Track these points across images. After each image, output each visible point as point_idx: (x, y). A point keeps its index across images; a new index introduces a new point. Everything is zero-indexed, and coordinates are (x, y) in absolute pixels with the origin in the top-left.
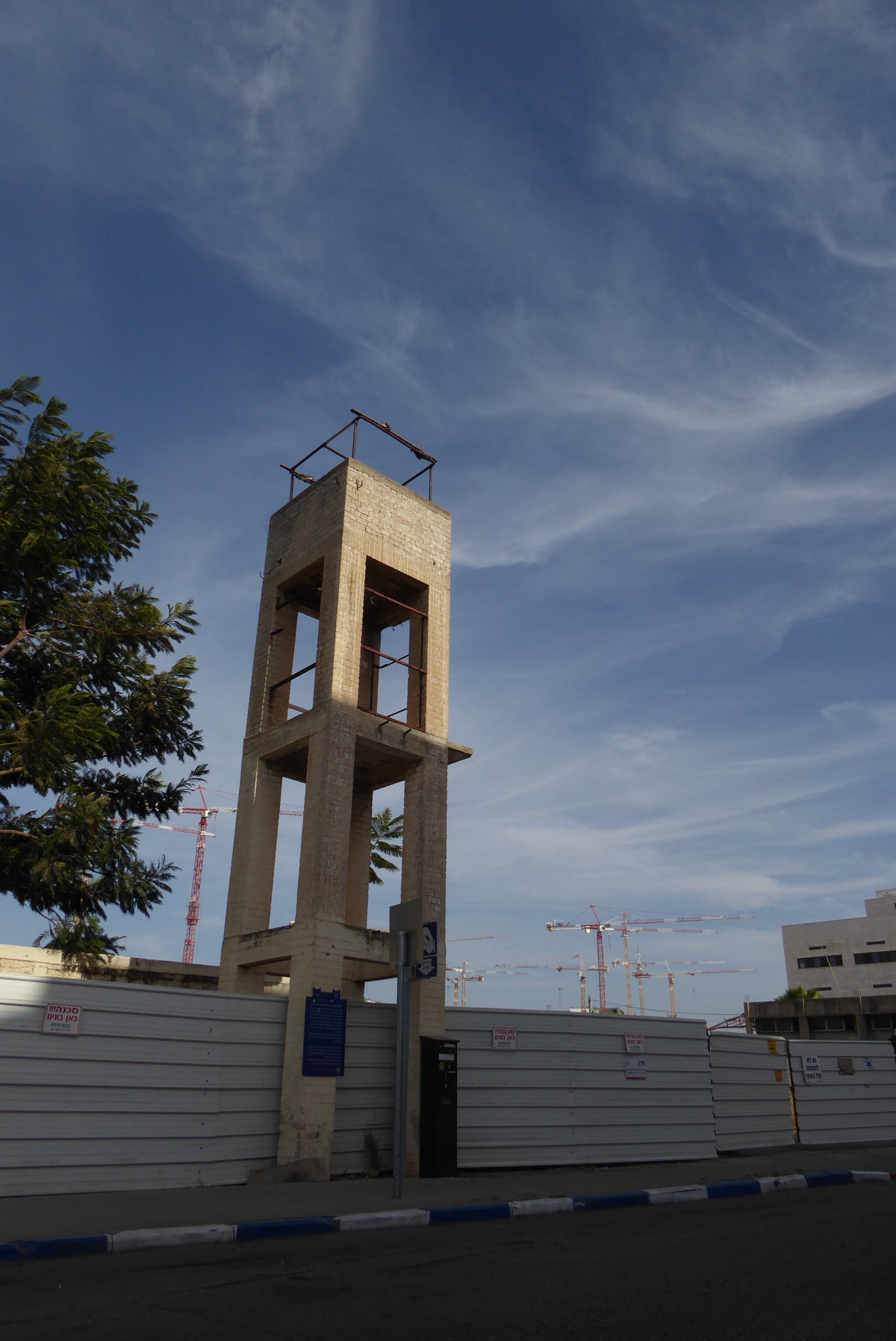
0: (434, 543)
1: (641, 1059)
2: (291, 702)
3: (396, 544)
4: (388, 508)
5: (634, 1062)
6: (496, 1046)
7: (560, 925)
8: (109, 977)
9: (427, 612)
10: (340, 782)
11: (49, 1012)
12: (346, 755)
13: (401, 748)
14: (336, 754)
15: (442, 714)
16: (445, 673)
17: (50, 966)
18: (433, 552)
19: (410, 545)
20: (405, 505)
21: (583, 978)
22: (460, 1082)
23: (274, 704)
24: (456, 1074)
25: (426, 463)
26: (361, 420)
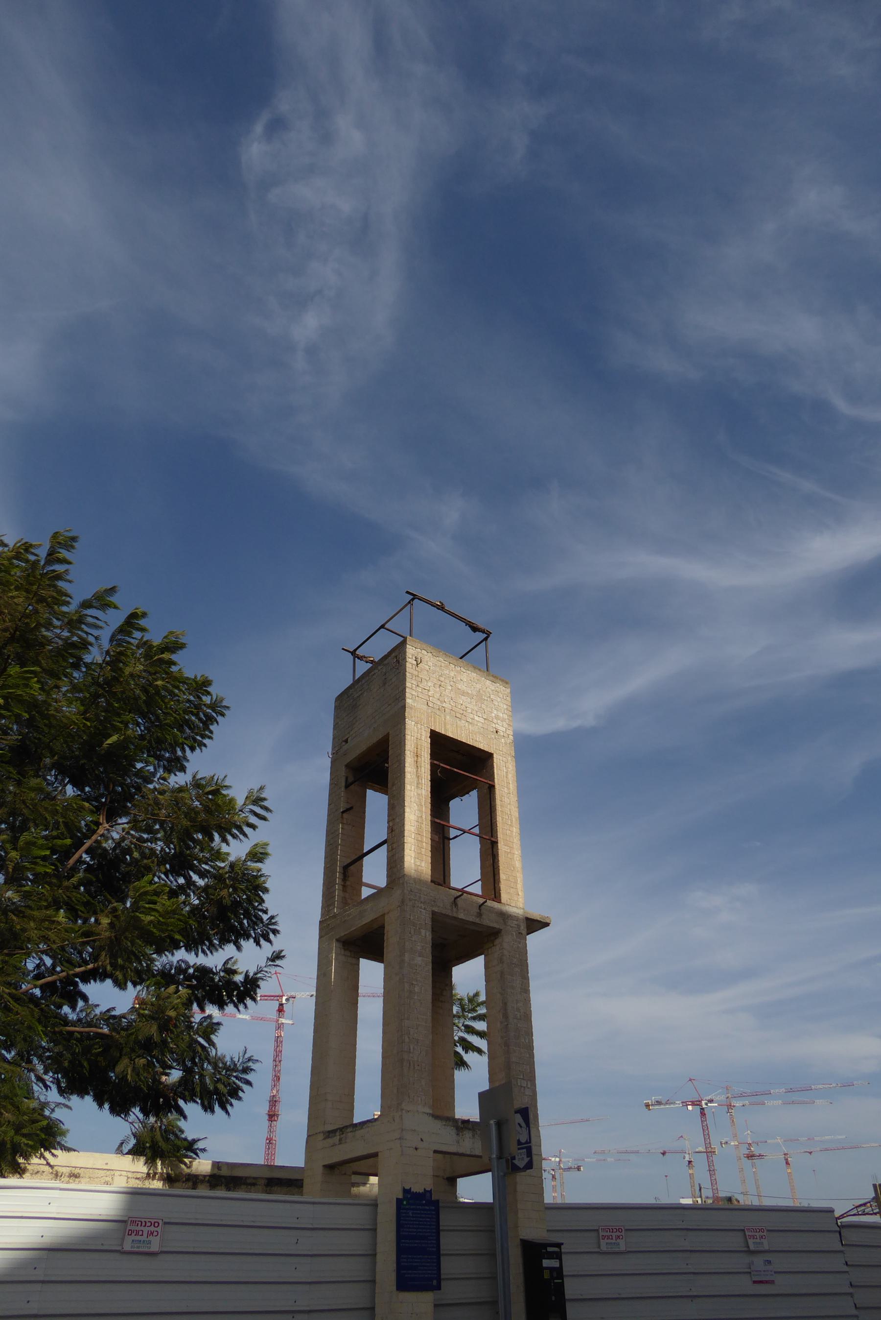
0: (495, 712)
2: (364, 880)
3: (459, 716)
4: (447, 681)
5: (758, 1262)
6: (604, 1248)
7: (659, 1103)
8: (190, 1184)
9: (493, 781)
10: (419, 960)
11: (129, 1228)
12: (423, 931)
13: (477, 921)
14: (412, 932)
15: (516, 883)
16: (516, 841)
17: (130, 1175)
18: (495, 721)
20: (464, 677)
21: (690, 1162)
22: (569, 1293)
23: (348, 883)
24: (562, 1284)
26: (416, 600)
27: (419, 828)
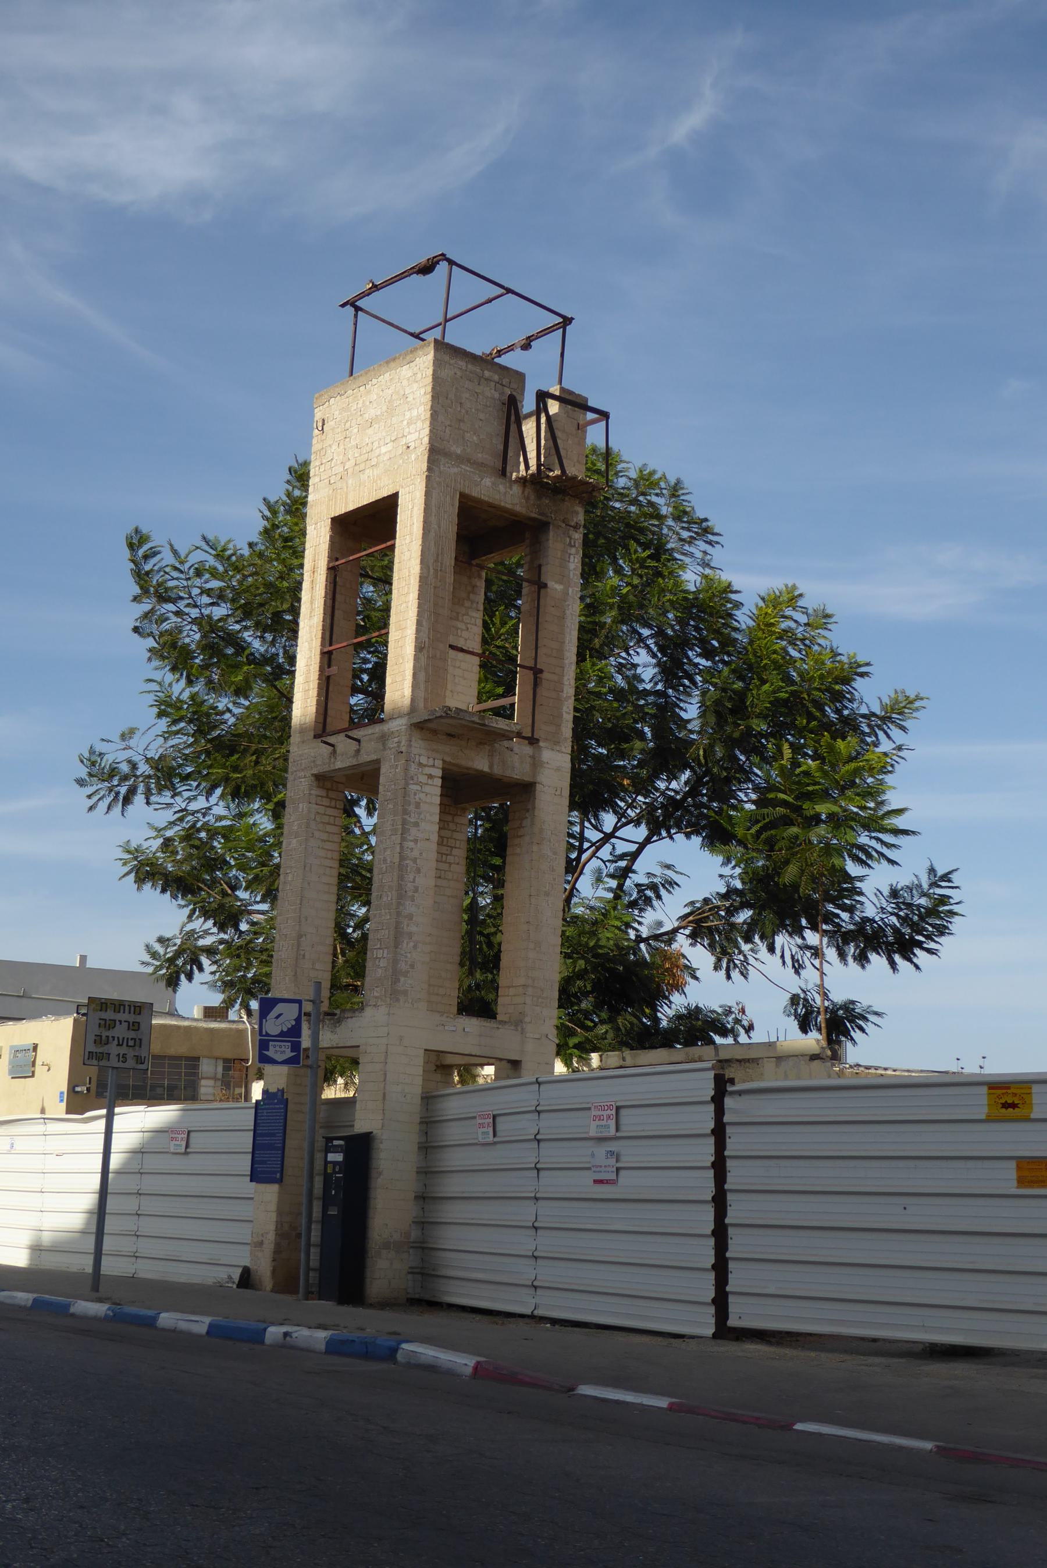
1: (614, 1146)
19: (377, 452)
27: (309, 671)
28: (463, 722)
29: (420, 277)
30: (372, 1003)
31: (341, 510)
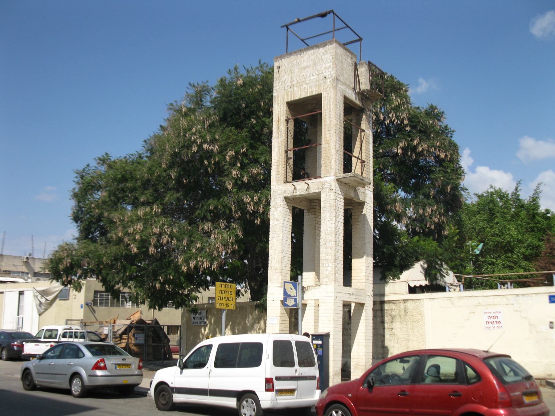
13: (307, 192)
19: (309, 78)
25: (330, 16)
27: (279, 158)
28: (356, 179)
29: (320, 18)
30: (324, 283)
31: (290, 99)
